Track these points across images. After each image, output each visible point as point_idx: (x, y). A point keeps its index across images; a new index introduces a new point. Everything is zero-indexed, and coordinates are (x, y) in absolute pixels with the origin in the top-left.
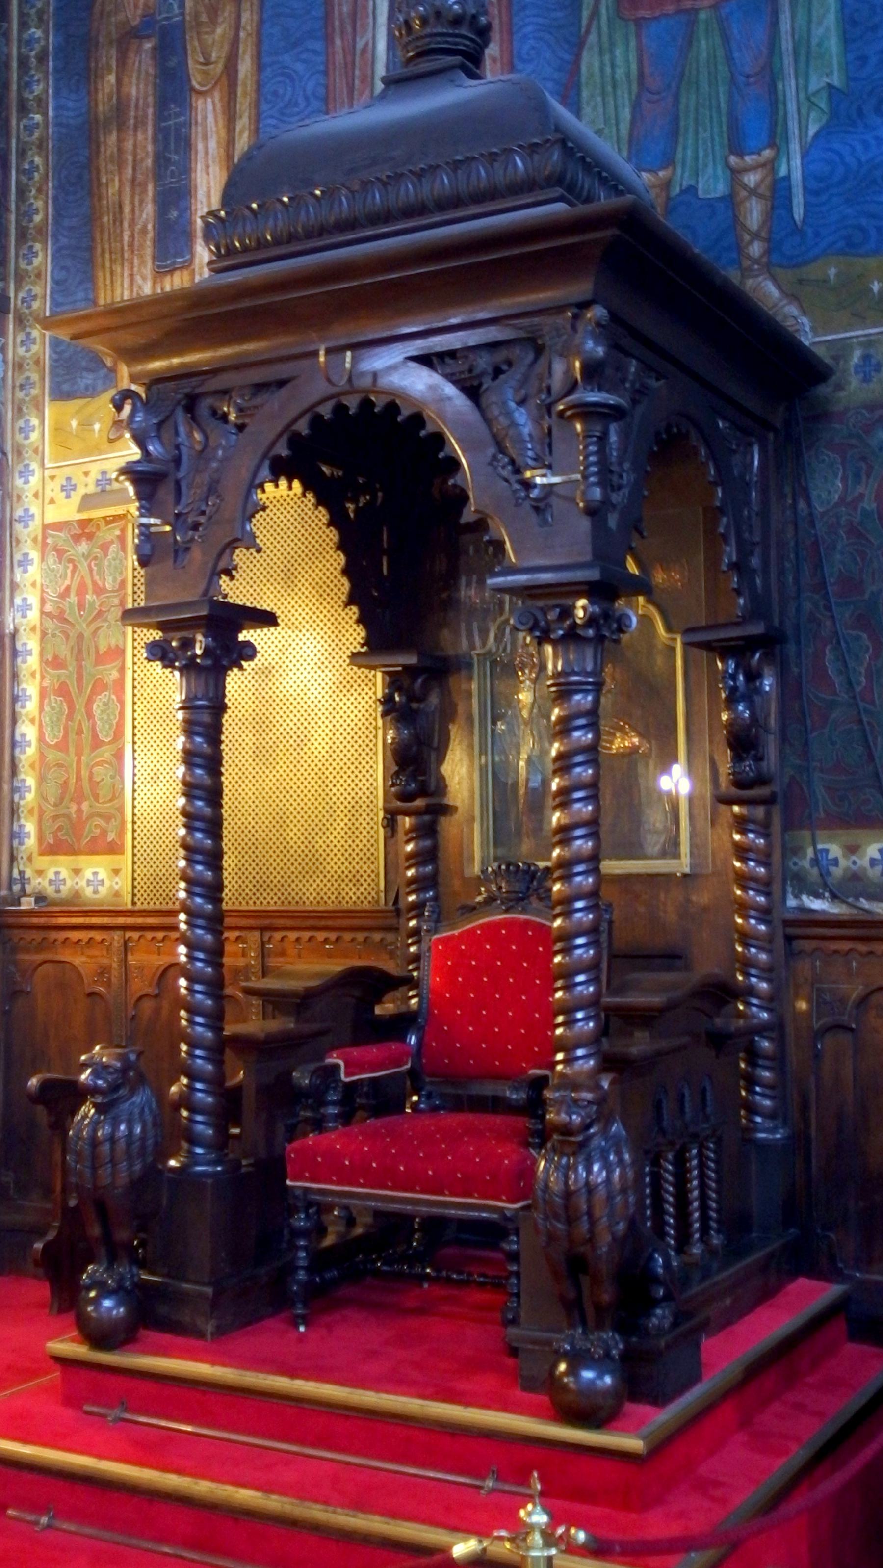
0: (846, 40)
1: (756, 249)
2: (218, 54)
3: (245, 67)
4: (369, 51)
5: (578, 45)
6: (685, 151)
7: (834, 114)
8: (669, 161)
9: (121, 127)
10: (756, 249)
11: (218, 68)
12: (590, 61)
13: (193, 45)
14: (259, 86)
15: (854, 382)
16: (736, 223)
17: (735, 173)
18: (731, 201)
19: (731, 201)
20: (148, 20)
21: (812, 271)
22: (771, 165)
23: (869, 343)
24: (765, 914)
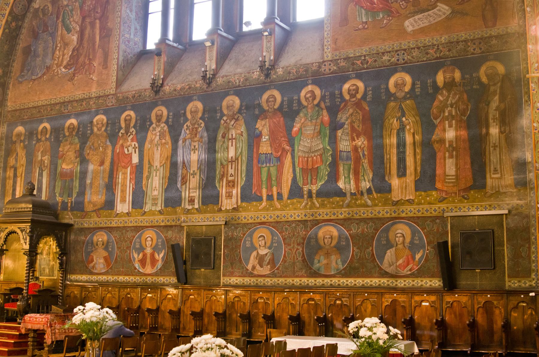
0: (79, 187)
1: (69, 209)
2: (21, 172)
3: (23, 175)
4: (36, 176)
5: (56, 181)
6: (64, 196)
7: (77, 195)
8: (63, 197)
9: (9, 179)
10: (69, 209)
11: (20, 174)
12: (57, 183)
13: (18, 171)
14: (25, 177)
15: (76, 225)
16: (68, 205)
17: (68, 200)
18: (67, 203)
19: (67, 202)
20: (13, 165)
21: (73, 212)
22: (71, 199)
23: (77, 221)
24: (62, 283)
